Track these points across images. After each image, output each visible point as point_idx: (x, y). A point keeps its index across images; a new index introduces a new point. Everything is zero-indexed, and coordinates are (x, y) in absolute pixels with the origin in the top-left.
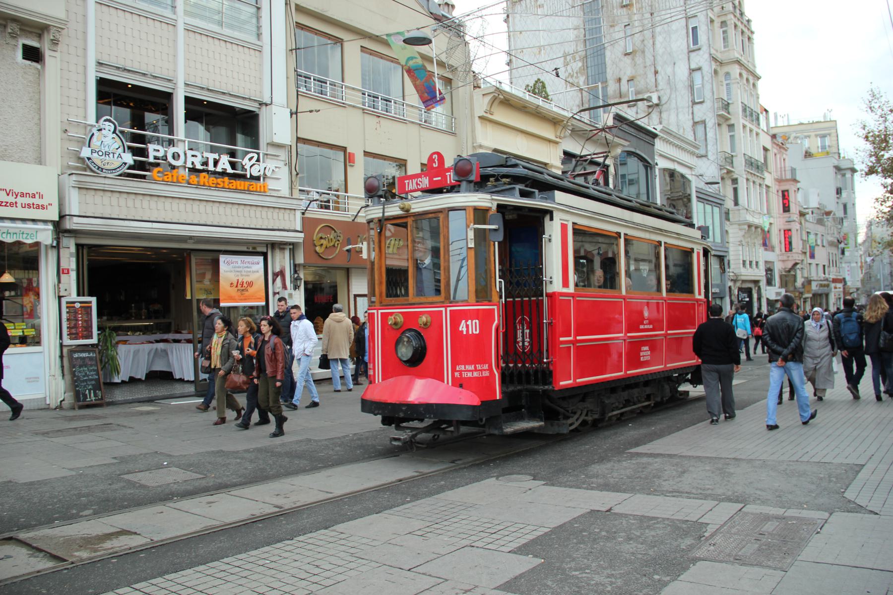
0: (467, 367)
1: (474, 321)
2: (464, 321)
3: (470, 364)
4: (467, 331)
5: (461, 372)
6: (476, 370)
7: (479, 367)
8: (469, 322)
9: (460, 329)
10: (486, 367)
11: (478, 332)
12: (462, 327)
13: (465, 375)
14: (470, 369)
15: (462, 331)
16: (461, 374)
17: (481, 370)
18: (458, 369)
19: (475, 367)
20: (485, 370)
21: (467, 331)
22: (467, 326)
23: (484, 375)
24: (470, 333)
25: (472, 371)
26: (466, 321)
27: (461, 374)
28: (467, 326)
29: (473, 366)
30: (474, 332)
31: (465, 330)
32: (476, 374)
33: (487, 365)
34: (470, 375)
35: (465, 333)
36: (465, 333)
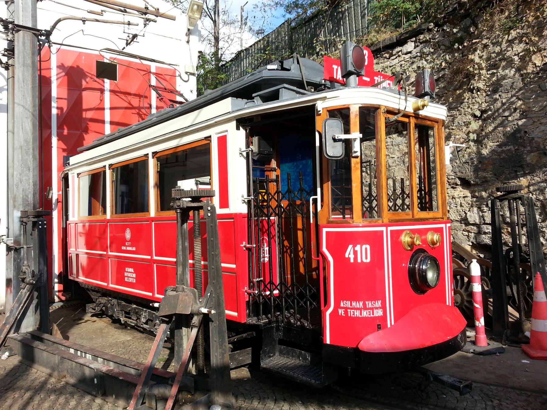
0: (354, 304)
1: (364, 247)
2: (351, 246)
3: (358, 300)
4: (356, 258)
5: (346, 309)
6: (365, 308)
7: (369, 304)
8: (358, 248)
9: (347, 256)
10: (379, 304)
11: (368, 260)
12: (349, 253)
13: (351, 313)
14: (358, 306)
15: (349, 258)
16: (346, 312)
17: (372, 309)
18: (342, 305)
19: (364, 304)
20: (377, 308)
21: (356, 258)
22: (355, 253)
23: (376, 315)
24: (359, 261)
25: (360, 309)
26: (354, 247)
27: (346, 312)
28: (355, 253)
29: (361, 303)
30: (364, 260)
31: (352, 257)
32: (365, 314)
33: (380, 302)
34: (357, 313)
35: (352, 261)
36: (352, 261)
